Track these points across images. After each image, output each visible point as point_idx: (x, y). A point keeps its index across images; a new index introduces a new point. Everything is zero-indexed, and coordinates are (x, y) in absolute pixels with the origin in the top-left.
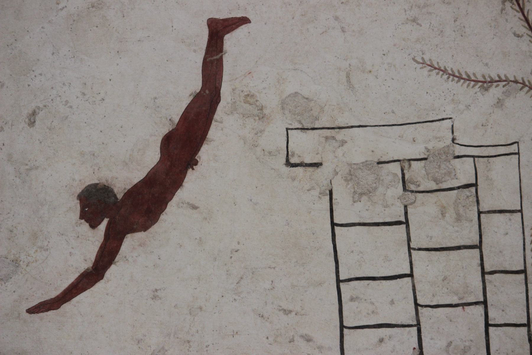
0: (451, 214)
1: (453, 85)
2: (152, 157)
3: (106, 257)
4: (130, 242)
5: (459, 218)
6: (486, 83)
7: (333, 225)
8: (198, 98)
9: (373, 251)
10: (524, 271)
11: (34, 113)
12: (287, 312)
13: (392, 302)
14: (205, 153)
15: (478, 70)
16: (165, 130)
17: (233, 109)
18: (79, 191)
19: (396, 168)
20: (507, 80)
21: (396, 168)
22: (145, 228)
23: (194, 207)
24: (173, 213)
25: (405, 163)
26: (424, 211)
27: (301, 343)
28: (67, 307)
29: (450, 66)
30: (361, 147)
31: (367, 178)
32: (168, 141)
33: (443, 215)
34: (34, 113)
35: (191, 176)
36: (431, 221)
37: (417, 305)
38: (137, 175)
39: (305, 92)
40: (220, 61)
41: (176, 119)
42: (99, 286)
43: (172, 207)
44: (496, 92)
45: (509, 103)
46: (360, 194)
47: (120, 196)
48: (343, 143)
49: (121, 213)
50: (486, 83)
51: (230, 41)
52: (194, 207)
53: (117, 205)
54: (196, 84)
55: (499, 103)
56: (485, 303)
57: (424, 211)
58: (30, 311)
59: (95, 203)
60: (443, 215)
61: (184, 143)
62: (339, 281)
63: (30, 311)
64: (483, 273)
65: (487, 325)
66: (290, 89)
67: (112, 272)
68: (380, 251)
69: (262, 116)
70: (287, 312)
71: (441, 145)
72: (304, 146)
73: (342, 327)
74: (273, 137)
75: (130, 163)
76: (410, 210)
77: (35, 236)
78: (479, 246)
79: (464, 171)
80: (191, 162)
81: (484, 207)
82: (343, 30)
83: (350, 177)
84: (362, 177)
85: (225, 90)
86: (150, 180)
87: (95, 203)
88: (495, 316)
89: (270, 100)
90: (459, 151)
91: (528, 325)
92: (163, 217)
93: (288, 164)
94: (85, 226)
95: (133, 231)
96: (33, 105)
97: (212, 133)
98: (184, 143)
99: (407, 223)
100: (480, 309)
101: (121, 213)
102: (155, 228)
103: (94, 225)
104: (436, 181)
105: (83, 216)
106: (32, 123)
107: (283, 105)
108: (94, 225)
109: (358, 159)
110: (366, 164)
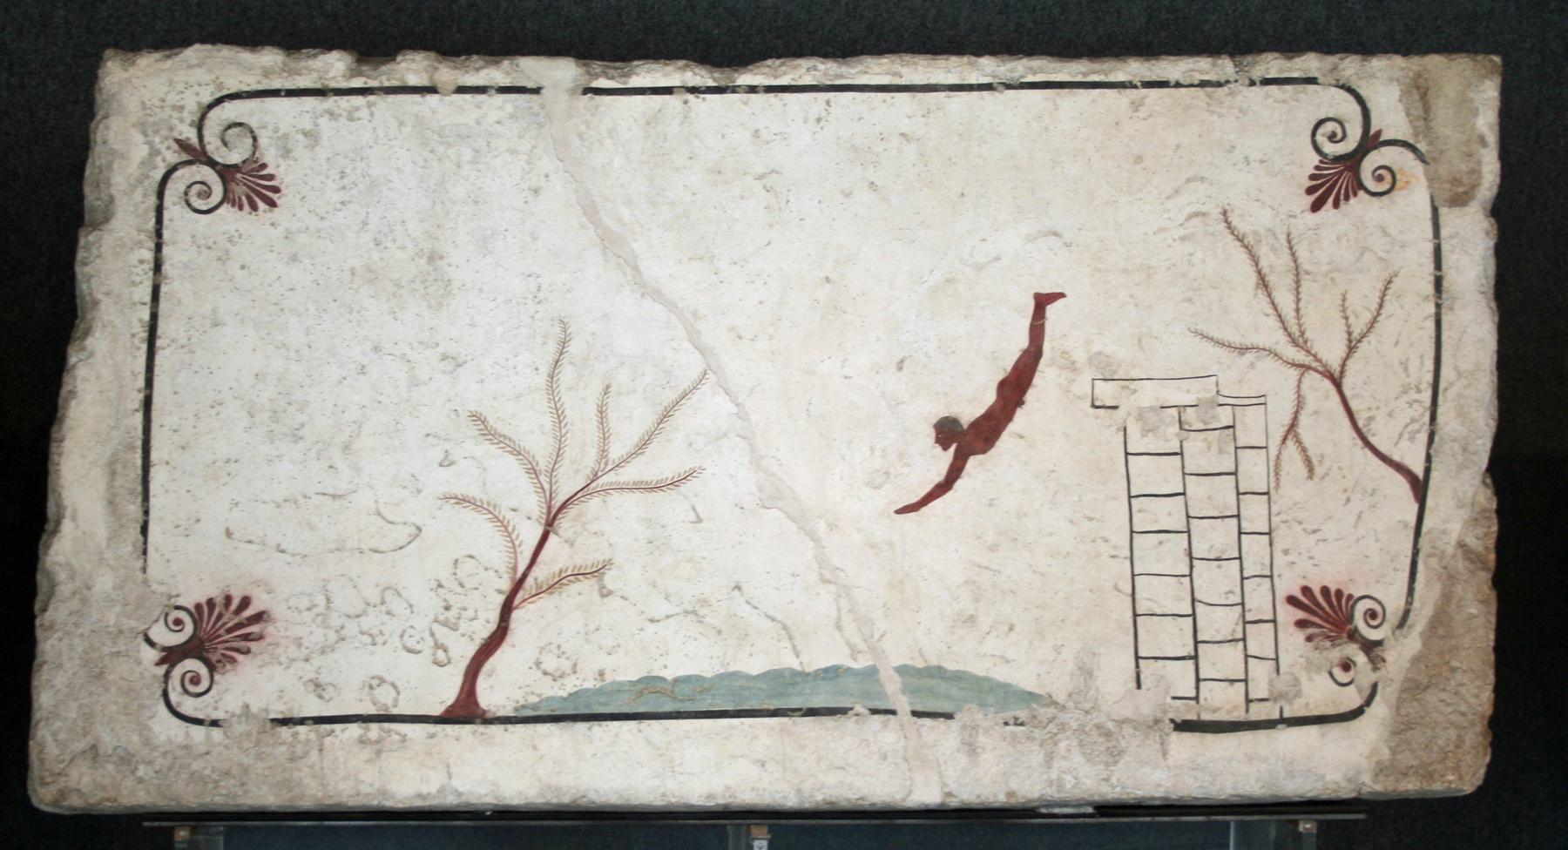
0: (1215, 448)
1: (1218, 350)
2: (990, 397)
3: (955, 473)
4: (973, 462)
5: (1221, 451)
6: (1243, 350)
7: (1127, 454)
8: (1025, 353)
9: (1157, 475)
10: (1267, 493)
11: (902, 361)
12: (1090, 519)
13: (1169, 514)
14: (1030, 396)
15: (1236, 339)
16: (1001, 376)
17: (1052, 362)
18: (934, 421)
19: (1174, 412)
20: (1258, 349)
21: (1174, 412)
22: (984, 451)
23: (1022, 437)
24: (1006, 441)
25: (1181, 408)
26: (1194, 445)
27: (1101, 543)
28: (924, 510)
29: (1216, 335)
30: (1148, 395)
31: (1153, 419)
32: (1002, 385)
33: (1209, 448)
34: (902, 361)
35: (1020, 414)
36: (1200, 453)
37: (1188, 517)
38: (979, 411)
39: (1109, 350)
40: (1042, 327)
41: (1009, 369)
42: (949, 495)
43: (1005, 436)
44: (1250, 356)
45: (1259, 365)
46: (1147, 431)
47: (965, 427)
48: (1135, 391)
49: (966, 439)
50: (1243, 350)
51: (1051, 310)
52: (1022, 437)
53: (964, 433)
54: (1023, 341)
55: (1252, 365)
56: (1238, 516)
57: (1194, 445)
58: (899, 512)
59: (947, 431)
60: (1209, 448)
61: (1015, 387)
62: (1130, 497)
63: (899, 512)
64: (1238, 494)
65: (1240, 533)
66: (1096, 348)
67: (959, 484)
68: (1163, 476)
69: (1073, 367)
70: (1090, 519)
71: (1208, 395)
72: (1106, 392)
73: (1132, 532)
74: (1083, 385)
75: (973, 404)
76: (1185, 444)
77: (901, 455)
78: (1235, 473)
79: (1225, 416)
80: (1020, 402)
81: (1240, 444)
82: (1136, 305)
83: (1140, 417)
84: (1148, 419)
85: (1046, 347)
86: (988, 416)
87: (947, 431)
88: (1246, 527)
89: (1080, 357)
90: (1222, 400)
91: (1269, 534)
92: (998, 443)
93: (1094, 406)
94: (939, 449)
95: (974, 453)
96: (900, 356)
97: (1037, 380)
98: (1015, 387)
99: (1181, 454)
100: (1235, 521)
101: (966, 439)
102: (992, 452)
103: (945, 448)
104: (1205, 423)
105: (938, 441)
106: (900, 369)
107: (1090, 360)
108: (945, 448)
109: (1146, 404)
110: (1152, 408)
